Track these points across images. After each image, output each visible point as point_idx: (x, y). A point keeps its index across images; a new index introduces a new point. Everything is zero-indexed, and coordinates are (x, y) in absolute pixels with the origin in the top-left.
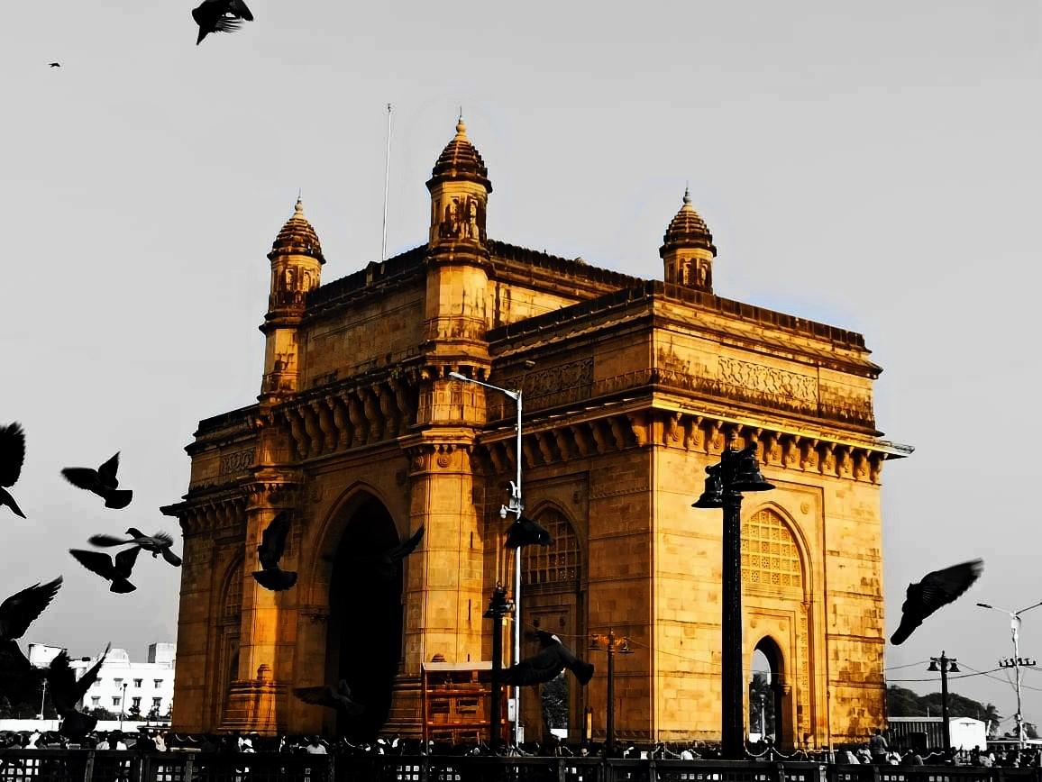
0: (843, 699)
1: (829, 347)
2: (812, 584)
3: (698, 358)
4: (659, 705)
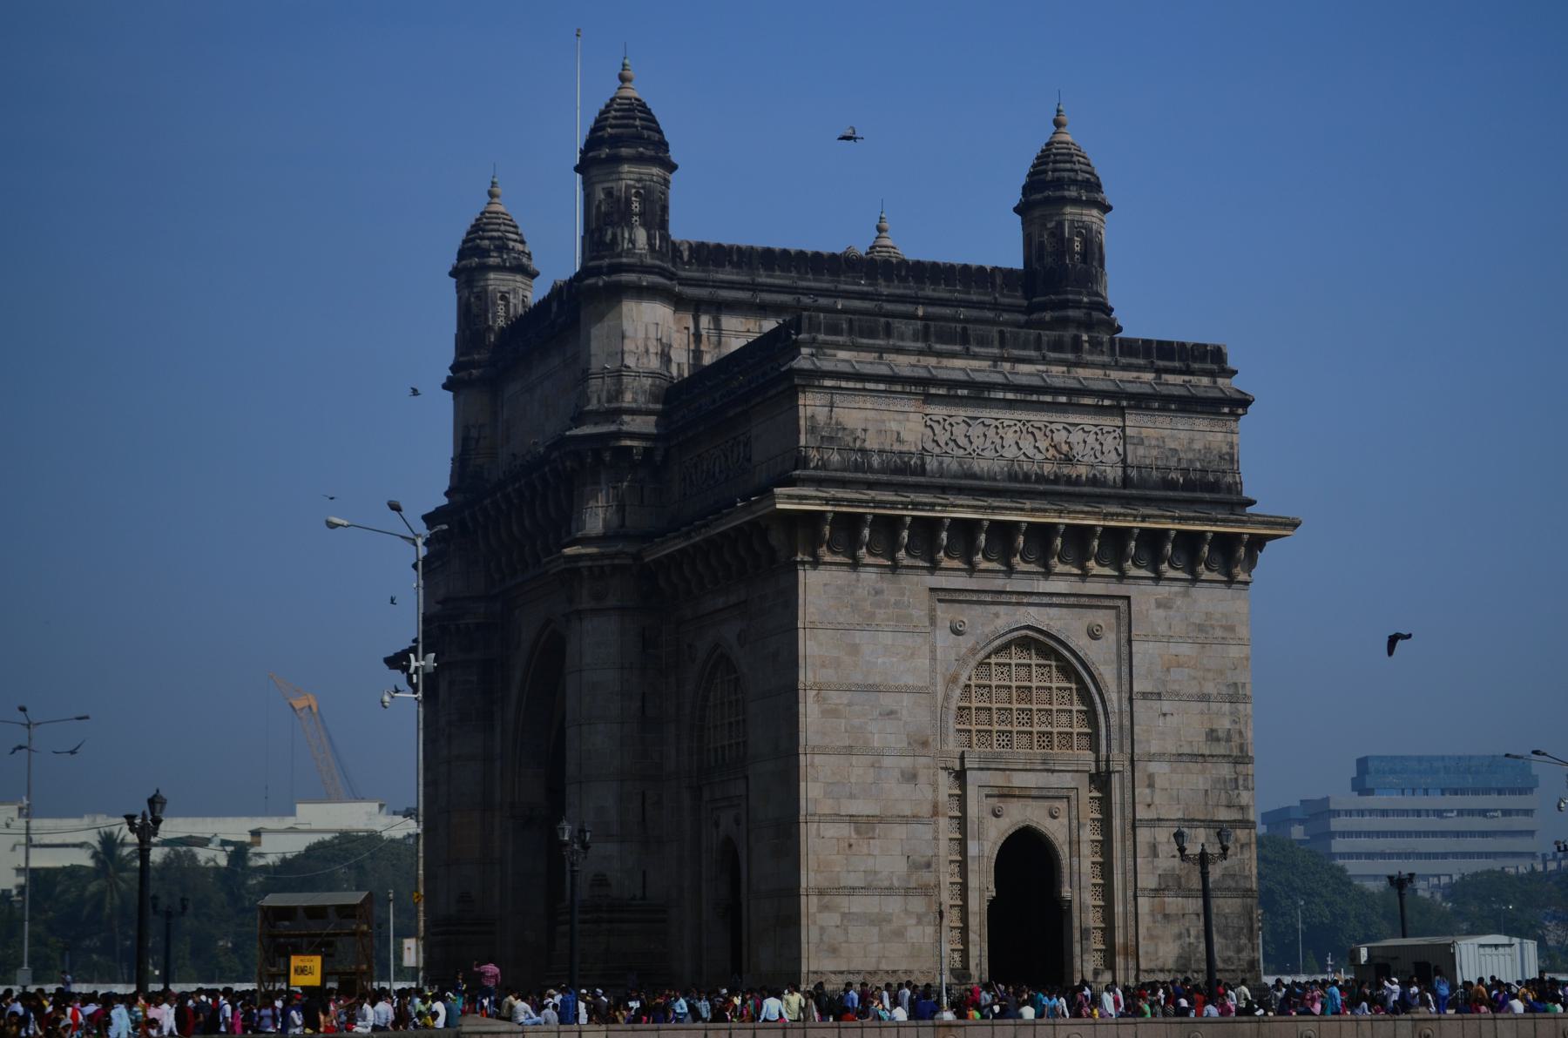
0: (1166, 916)
1: (1149, 376)
2: (1109, 746)
3: (884, 421)
4: (810, 935)
